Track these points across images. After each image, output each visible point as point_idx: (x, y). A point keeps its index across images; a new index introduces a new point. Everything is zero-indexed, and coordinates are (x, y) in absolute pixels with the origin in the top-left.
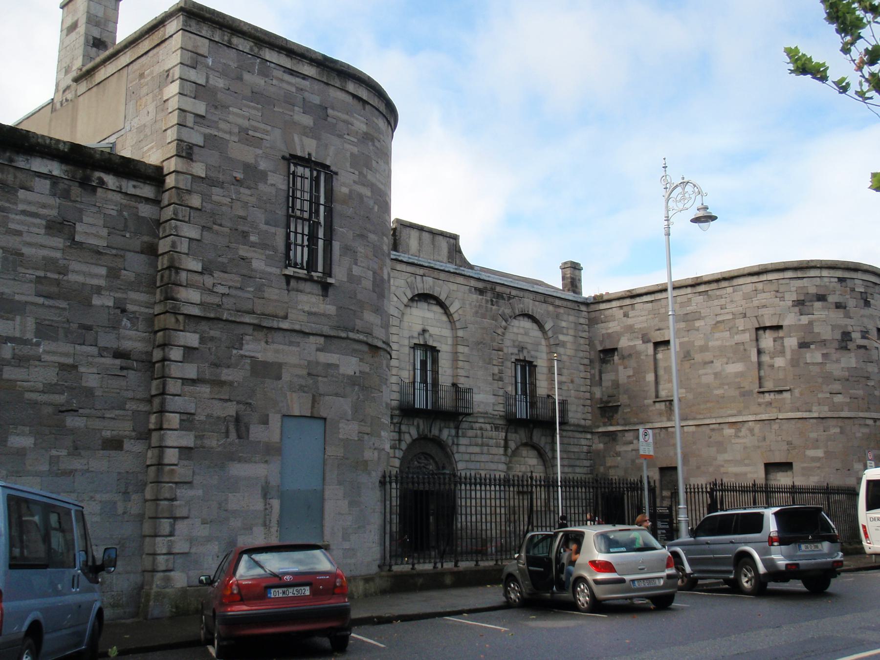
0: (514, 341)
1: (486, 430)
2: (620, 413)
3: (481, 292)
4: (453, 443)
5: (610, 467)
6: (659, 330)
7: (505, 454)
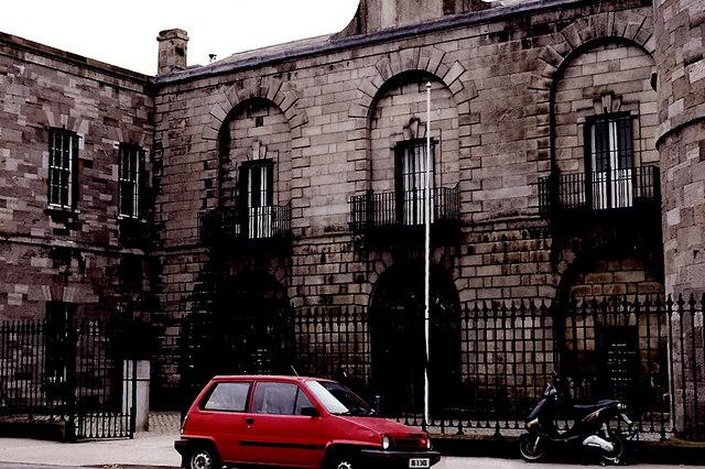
0: (584, 89)
1: (514, 239)
3: (503, 36)
7: (554, 271)
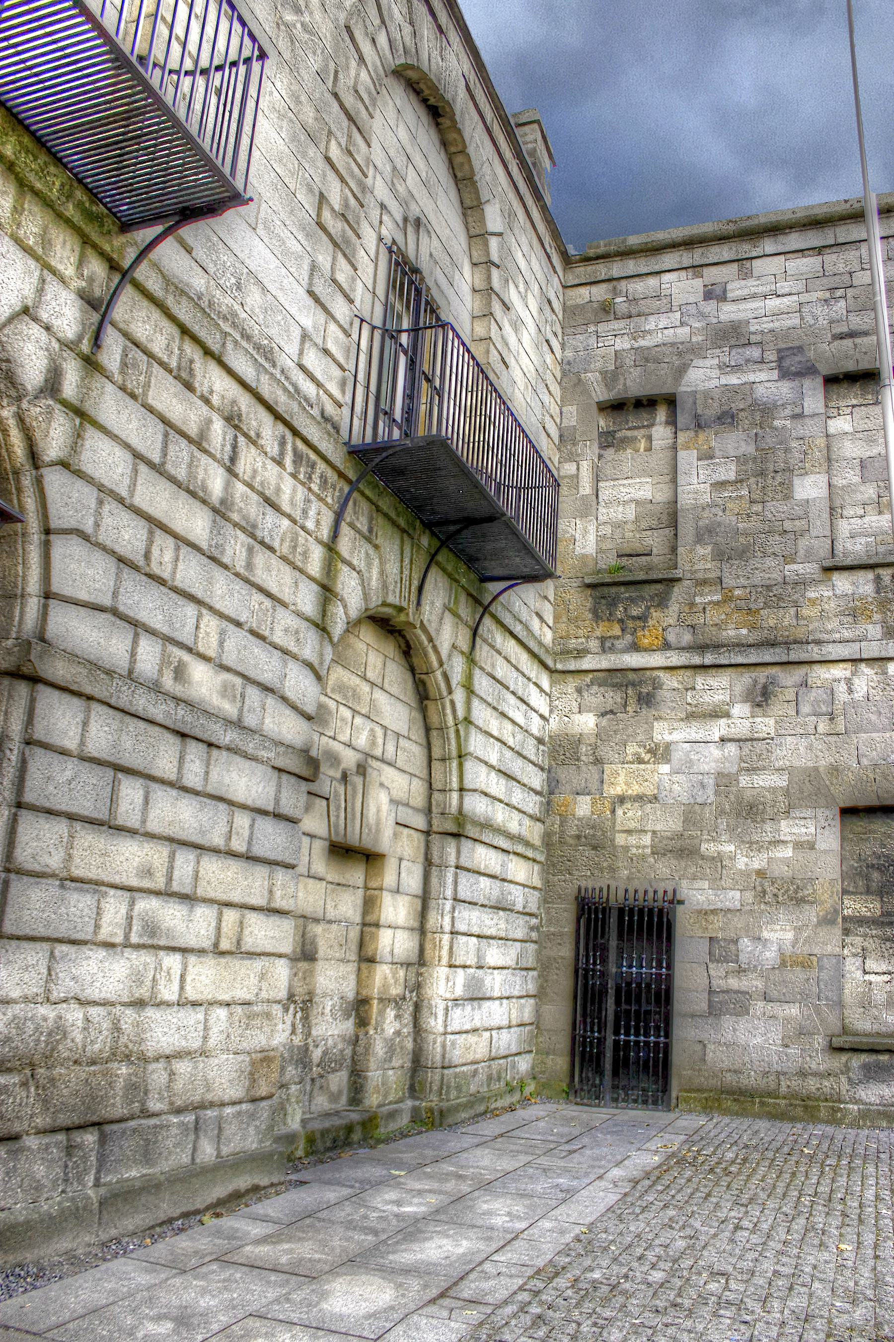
2: (674, 608)
4: (52, 386)
5: (622, 800)
6: (852, 335)
